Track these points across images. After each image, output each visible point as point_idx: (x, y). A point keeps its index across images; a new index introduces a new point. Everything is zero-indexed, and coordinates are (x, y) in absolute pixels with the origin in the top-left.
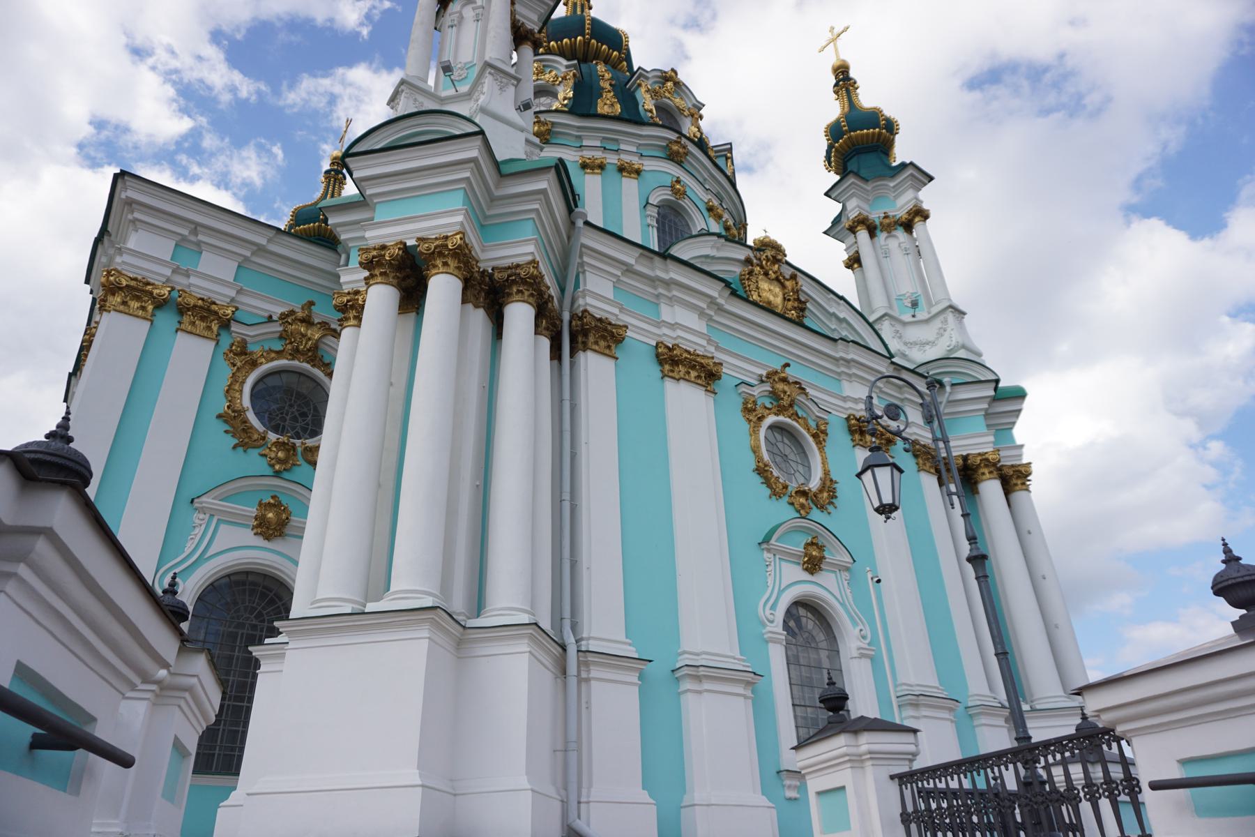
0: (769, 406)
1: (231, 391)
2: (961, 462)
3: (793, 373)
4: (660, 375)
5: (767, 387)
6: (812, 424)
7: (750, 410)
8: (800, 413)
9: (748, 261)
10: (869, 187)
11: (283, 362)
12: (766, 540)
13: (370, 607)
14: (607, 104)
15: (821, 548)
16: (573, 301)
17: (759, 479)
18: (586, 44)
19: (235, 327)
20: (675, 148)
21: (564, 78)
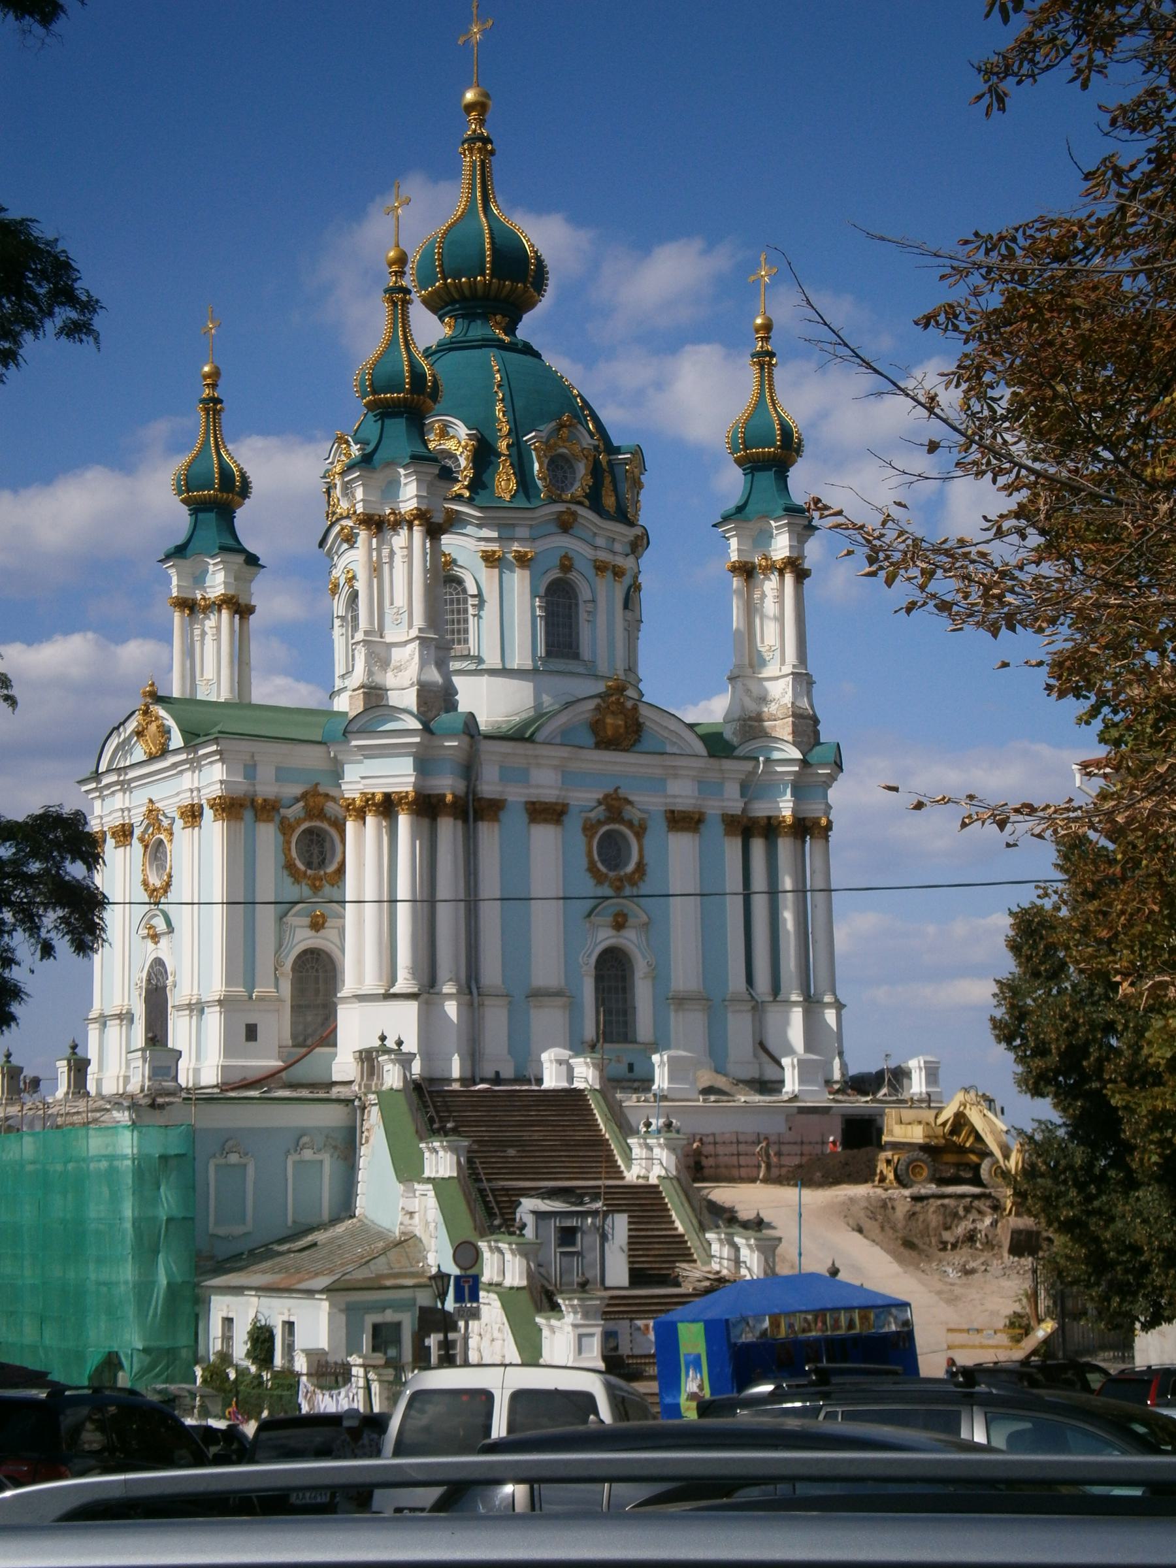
0: (602, 818)
1: (286, 851)
2: (763, 822)
3: (622, 793)
4: (527, 820)
5: (603, 807)
6: (636, 823)
7: (589, 829)
8: (626, 816)
9: (598, 708)
10: (750, 525)
11: (306, 825)
12: (589, 915)
13: (392, 991)
14: (504, 483)
15: (625, 916)
16: (475, 786)
17: (588, 875)
18: (487, 286)
19: (282, 811)
20: (566, 517)
21: (465, 447)
